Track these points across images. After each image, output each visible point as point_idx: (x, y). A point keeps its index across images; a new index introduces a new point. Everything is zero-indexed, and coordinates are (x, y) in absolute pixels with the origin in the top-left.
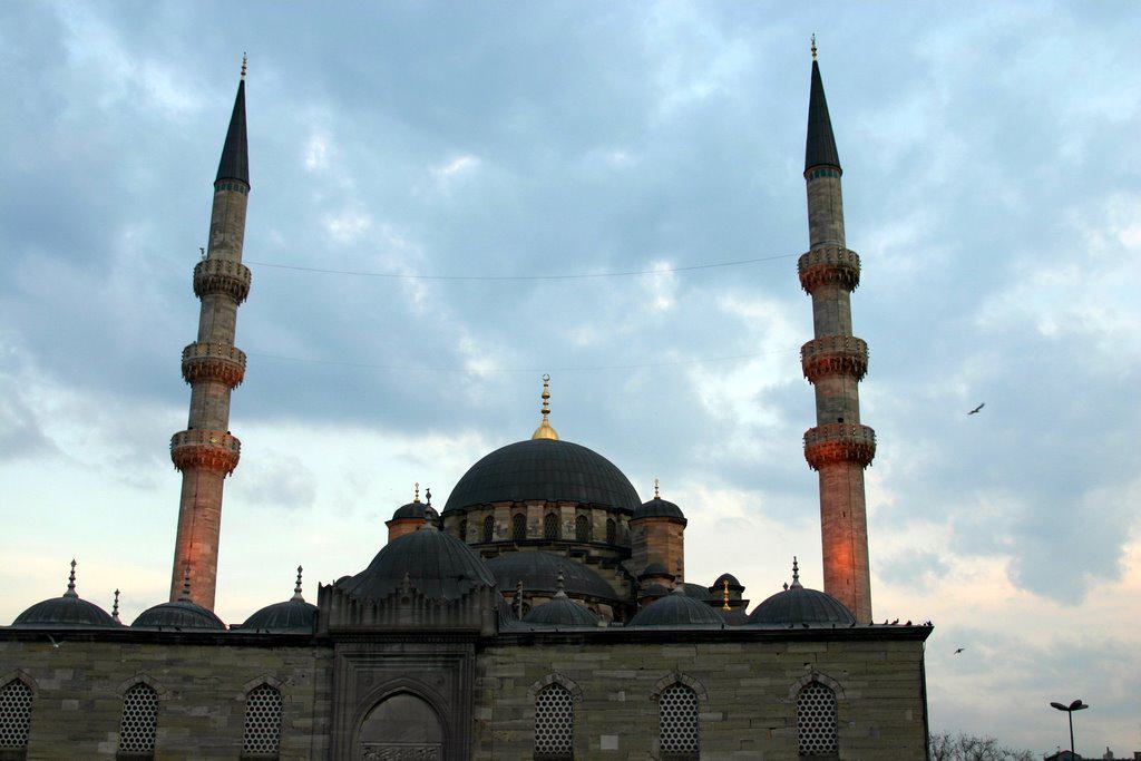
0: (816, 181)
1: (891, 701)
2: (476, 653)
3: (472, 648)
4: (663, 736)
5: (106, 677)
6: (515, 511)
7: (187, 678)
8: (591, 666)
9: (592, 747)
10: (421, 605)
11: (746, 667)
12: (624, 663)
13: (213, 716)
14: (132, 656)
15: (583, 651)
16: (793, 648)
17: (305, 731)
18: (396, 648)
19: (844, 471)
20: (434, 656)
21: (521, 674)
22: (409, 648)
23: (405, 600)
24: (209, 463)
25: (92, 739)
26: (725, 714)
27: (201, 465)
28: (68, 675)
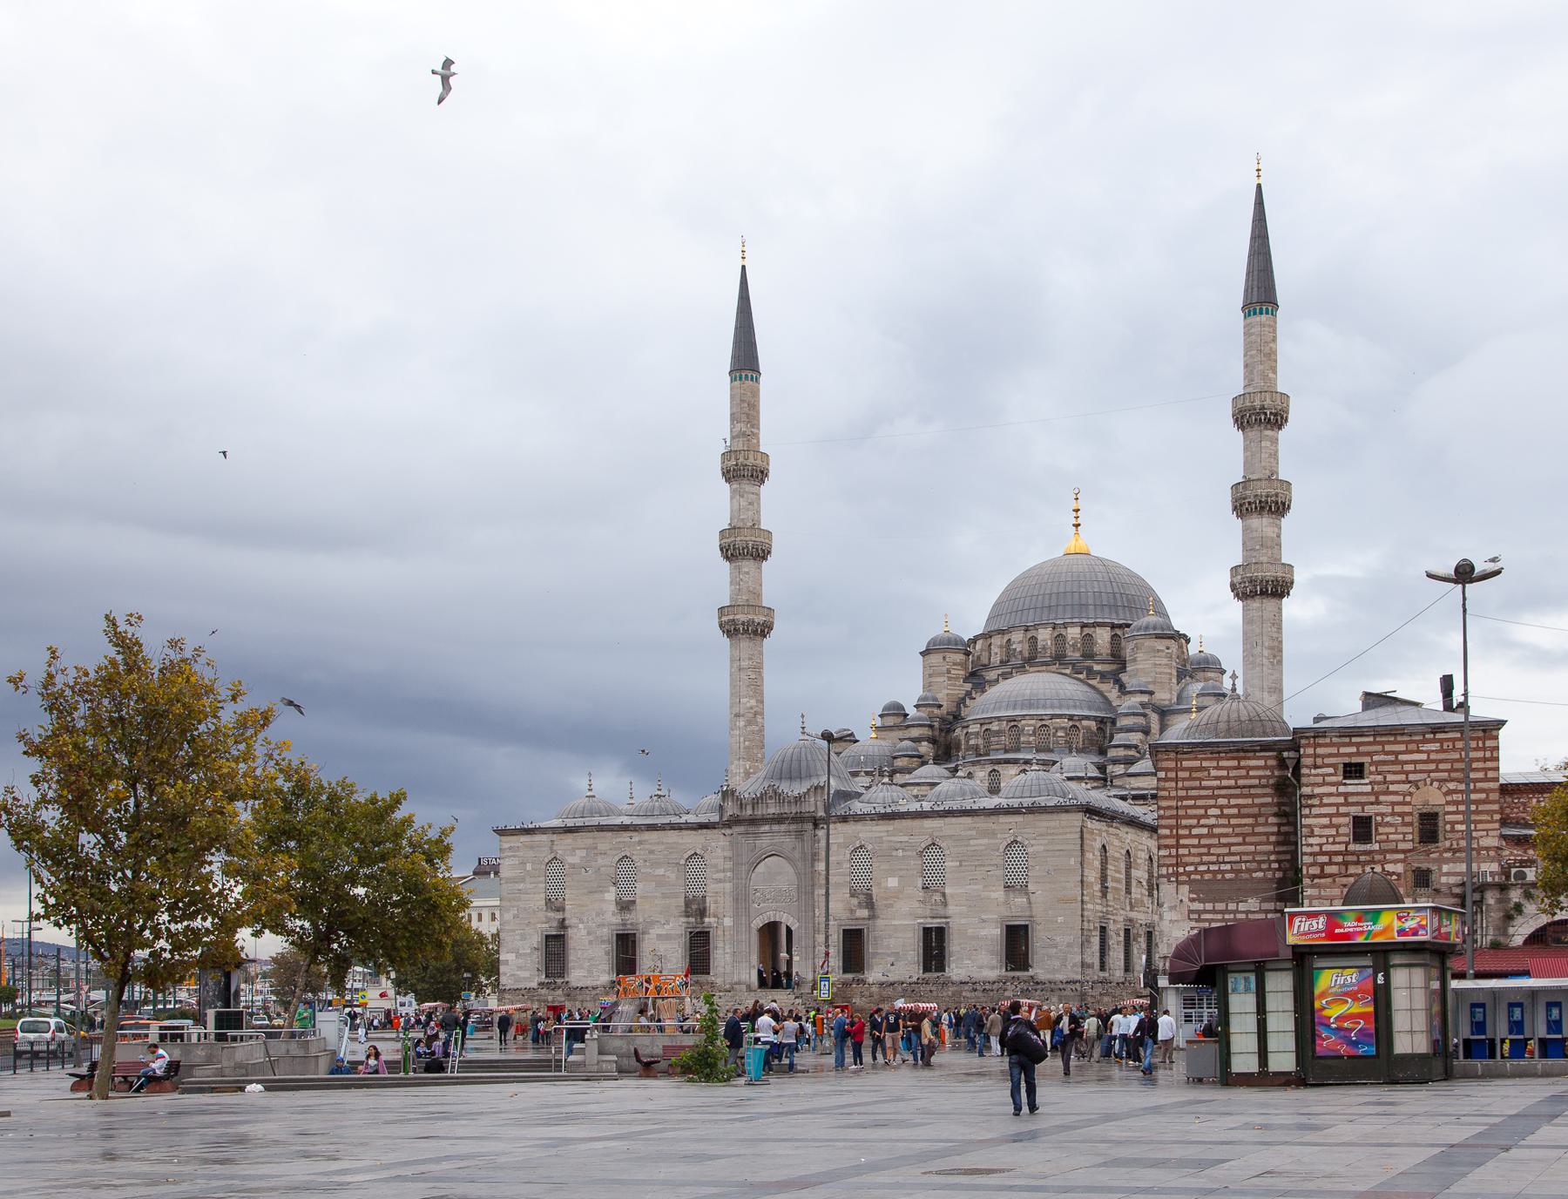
0: (1250, 320)
1: (1061, 852)
2: (814, 829)
3: (810, 826)
4: (925, 877)
5: (605, 854)
6: (1029, 635)
7: (651, 852)
8: (882, 834)
9: (883, 885)
10: (779, 800)
11: (974, 833)
12: (901, 832)
13: (668, 874)
14: (618, 840)
15: (877, 825)
16: (1003, 819)
17: (720, 881)
18: (767, 828)
19: (1258, 605)
20: (789, 832)
21: (842, 841)
22: (775, 827)
23: (771, 798)
24: (746, 631)
25: (601, 891)
26: (960, 861)
27: (742, 634)
28: (583, 853)
